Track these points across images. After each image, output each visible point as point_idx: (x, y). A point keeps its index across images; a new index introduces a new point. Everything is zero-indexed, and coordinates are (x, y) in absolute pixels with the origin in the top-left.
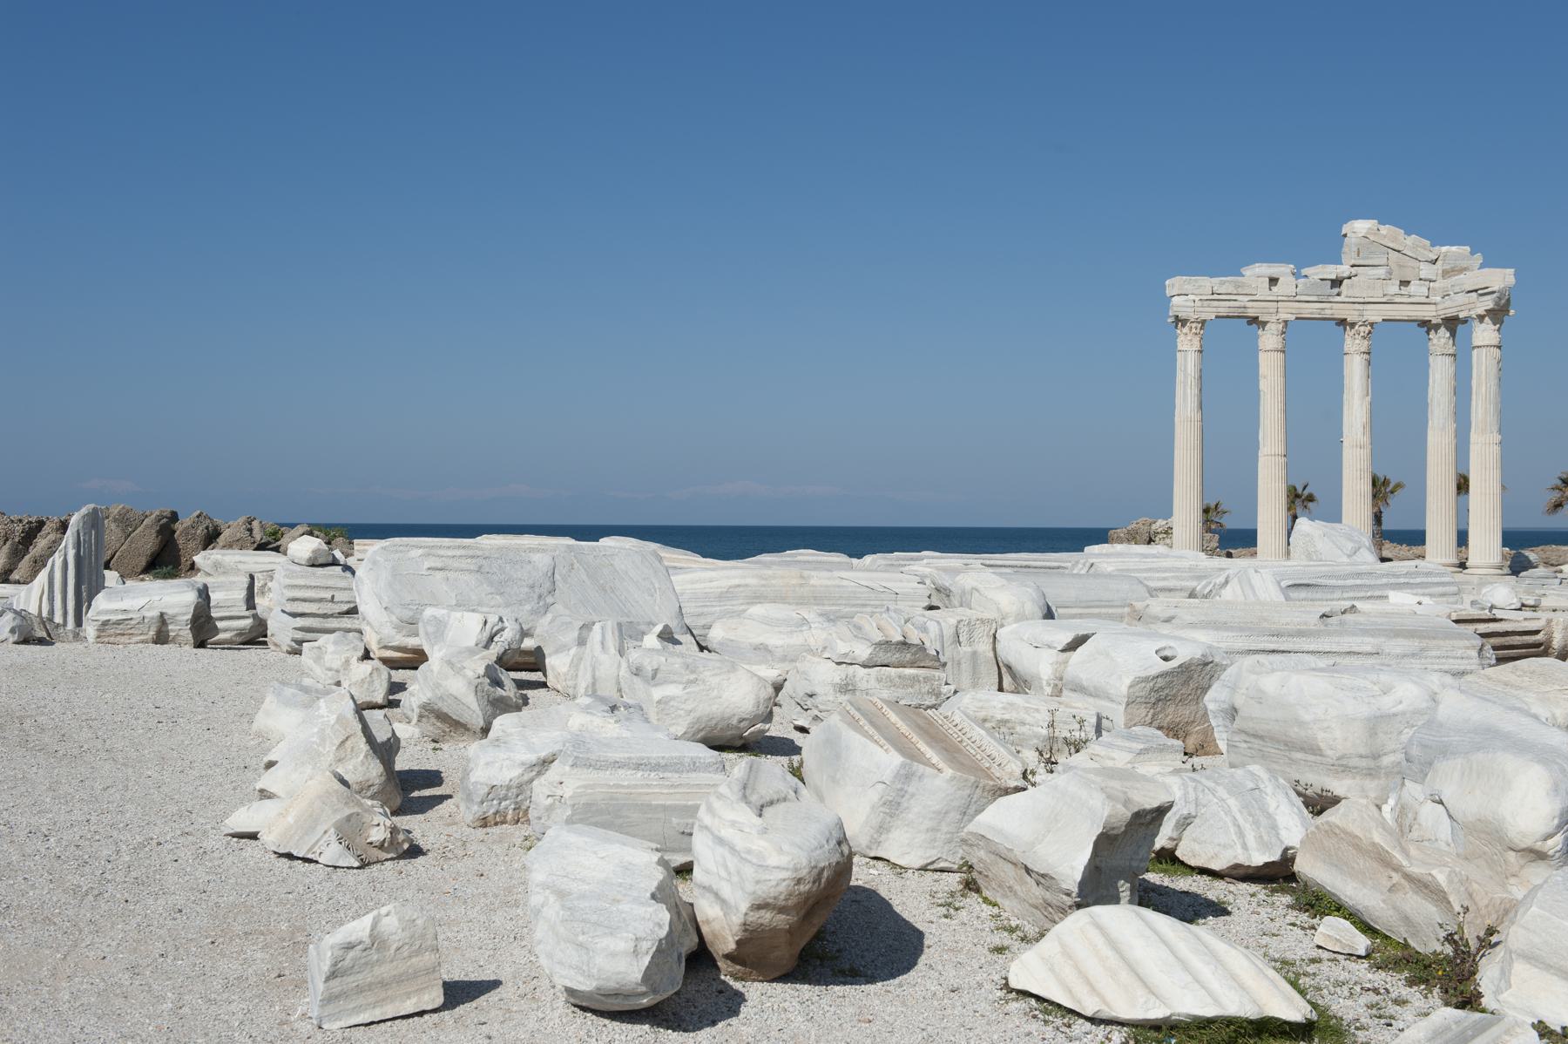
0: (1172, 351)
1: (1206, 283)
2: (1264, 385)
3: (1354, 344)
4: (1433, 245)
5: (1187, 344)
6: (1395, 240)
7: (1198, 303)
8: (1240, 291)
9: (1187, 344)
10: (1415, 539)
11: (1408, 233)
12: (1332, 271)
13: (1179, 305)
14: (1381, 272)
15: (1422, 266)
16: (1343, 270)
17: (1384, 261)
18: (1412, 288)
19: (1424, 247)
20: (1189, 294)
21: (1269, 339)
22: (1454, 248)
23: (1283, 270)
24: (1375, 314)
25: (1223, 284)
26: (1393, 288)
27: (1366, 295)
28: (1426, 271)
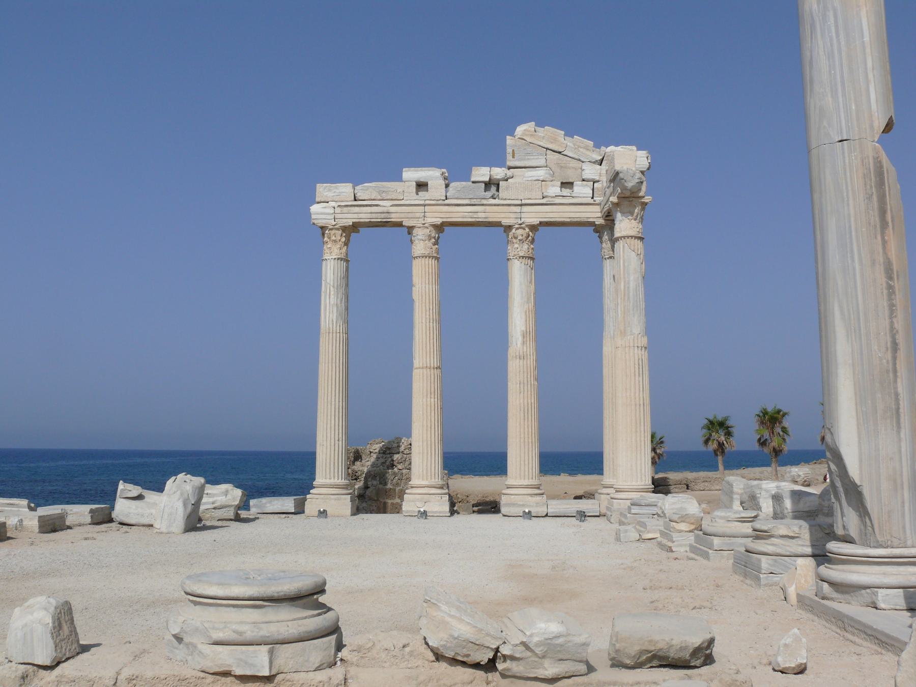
0: (318, 261)
1: (345, 190)
2: (416, 295)
3: (518, 248)
4: (597, 146)
5: (332, 252)
6: (554, 140)
7: (338, 210)
8: (384, 196)
9: (332, 252)
10: (590, 462)
11: (569, 134)
12: (482, 173)
13: (320, 213)
14: (541, 173)
15: (585, 166)
16: (498, 172)
17: (542, 162)
18: (575, 188)
19: (587, 148)
20: (332, 203)
21: (421, 245)
22: (619, 148)
23: (433, 175)
24: (532, 216)
25: (367, 190)
26: (554, 189)
27: (525, 197)
28: (591, 171)
